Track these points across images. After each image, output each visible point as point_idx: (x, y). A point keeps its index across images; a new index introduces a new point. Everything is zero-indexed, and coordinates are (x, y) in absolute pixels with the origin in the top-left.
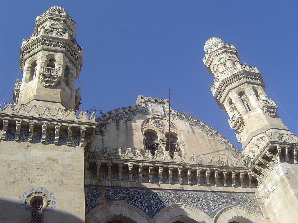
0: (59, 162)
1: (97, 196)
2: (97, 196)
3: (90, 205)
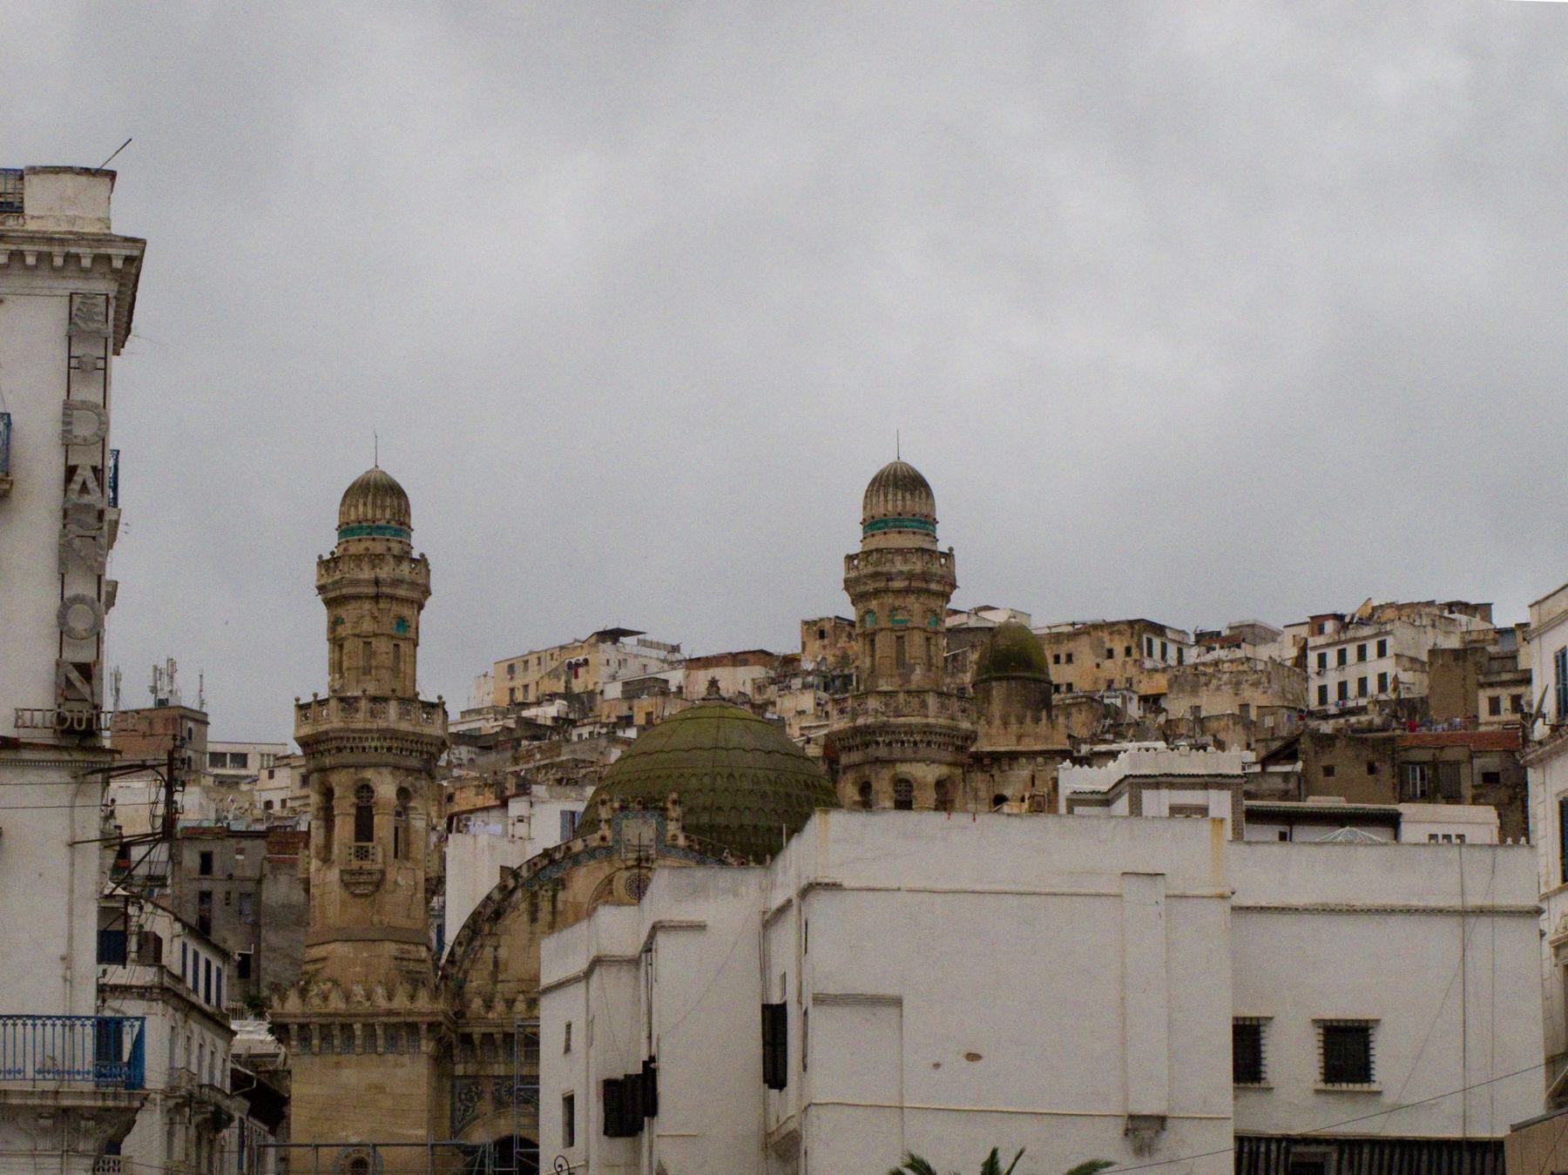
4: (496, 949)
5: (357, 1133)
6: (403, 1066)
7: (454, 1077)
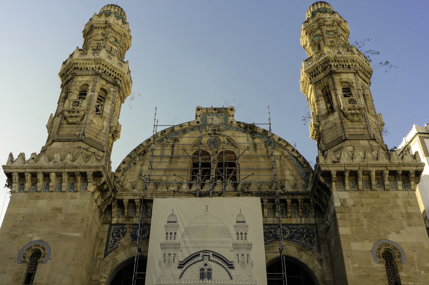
0: (63, 212)
1: (121, 236)
2: (121, 236)
3: (112, 246)
4: (142, 166)
5: (38, 235)
6: (75, 198)
7: (111, 225)
